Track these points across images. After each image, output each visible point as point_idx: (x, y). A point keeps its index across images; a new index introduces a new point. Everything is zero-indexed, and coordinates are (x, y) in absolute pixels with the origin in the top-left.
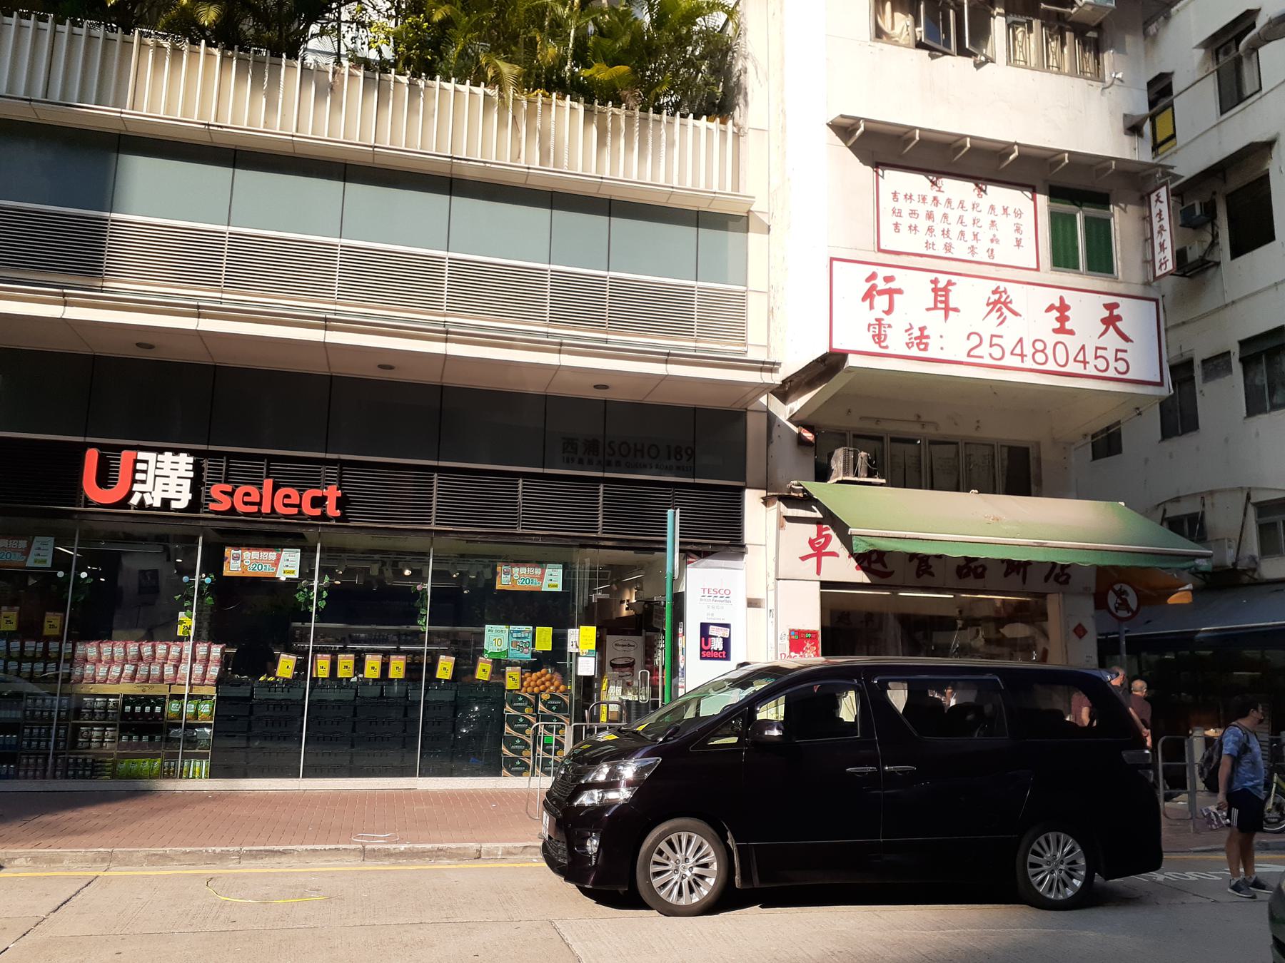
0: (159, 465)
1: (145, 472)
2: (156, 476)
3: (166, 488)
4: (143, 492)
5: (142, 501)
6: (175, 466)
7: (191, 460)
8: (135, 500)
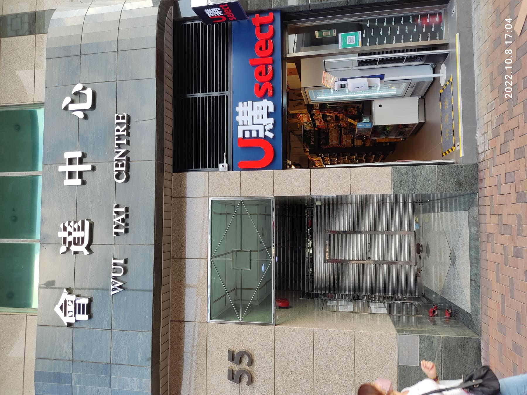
0: (245, 123)
1: (250, 131)
2: (253, 124)
3: (260, 117)
4: (265, 130)
5: (270, 131)
6: (245, 113)
7: (240, 104)
8: (271, 135)
